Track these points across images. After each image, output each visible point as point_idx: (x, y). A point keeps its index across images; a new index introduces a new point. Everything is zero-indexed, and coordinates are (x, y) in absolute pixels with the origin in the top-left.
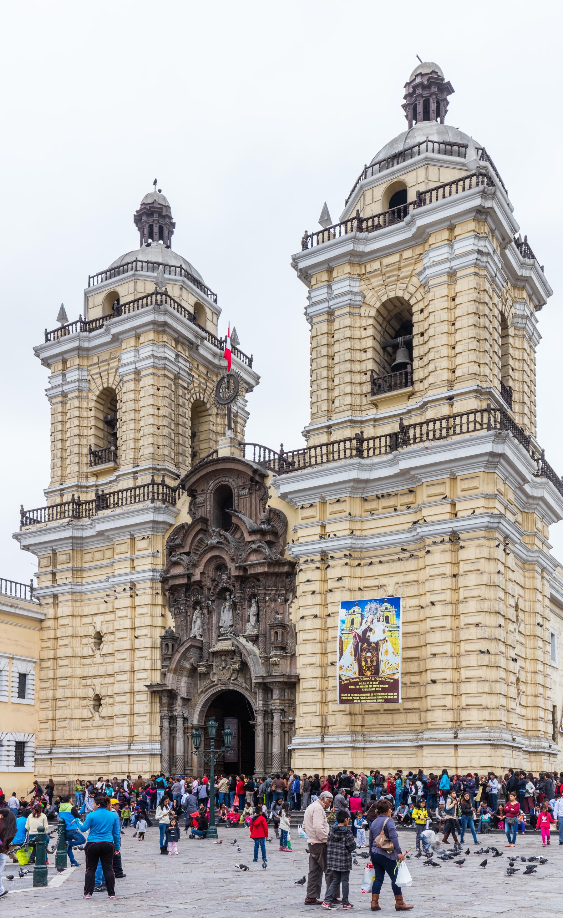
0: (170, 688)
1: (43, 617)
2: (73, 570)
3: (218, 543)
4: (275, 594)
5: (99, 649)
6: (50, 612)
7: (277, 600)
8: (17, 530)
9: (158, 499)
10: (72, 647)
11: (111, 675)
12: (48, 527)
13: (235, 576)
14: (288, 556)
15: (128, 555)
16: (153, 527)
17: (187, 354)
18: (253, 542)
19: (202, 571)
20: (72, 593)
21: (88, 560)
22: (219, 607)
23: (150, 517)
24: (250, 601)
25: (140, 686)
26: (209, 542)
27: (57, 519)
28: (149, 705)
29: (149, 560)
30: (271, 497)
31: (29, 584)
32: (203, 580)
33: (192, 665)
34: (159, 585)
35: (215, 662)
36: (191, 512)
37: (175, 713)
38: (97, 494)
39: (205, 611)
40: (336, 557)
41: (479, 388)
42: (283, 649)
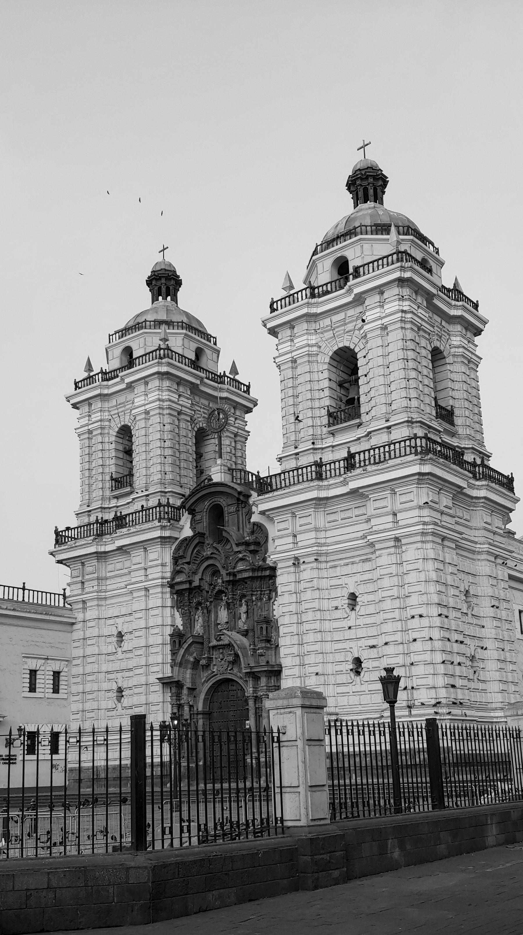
0: (176, 680)
1: (74, 621)
2: (98, 579)
3: (212, 554)
4: (261, 594)
5: (121, 647)
6: (80, 616)
7: (263, 599)
8: (52, 548)
9: (164, 518)
10: (98, 646)
11: (130, 670)
12: (77, 544)
13: (226, 581)
14: (269, 562)
15: (142, 565)
16: (161, 542)
17: (189, 393)
18: (240, 552)
19: (200, 578)
20: (99, 599)
21: (111, 570)
22: (216, 607)
23: (157, 533)
24: (241, 601)
25: (153, 679)
26: (205, 554)
27: (84, 537)
28: (162, 695)
29: (159, 569)
30: (254, 512)
31: (62, 592)
32: (202, 585)
33: (195, 658)
34: (168, 590)
35: (215, 655)
36: (193, 528)
37: (182, 702)
38: (116, 515)
39: (205, 611)
40: (306, 561)
41: (410, 419)
42: (269, 641)
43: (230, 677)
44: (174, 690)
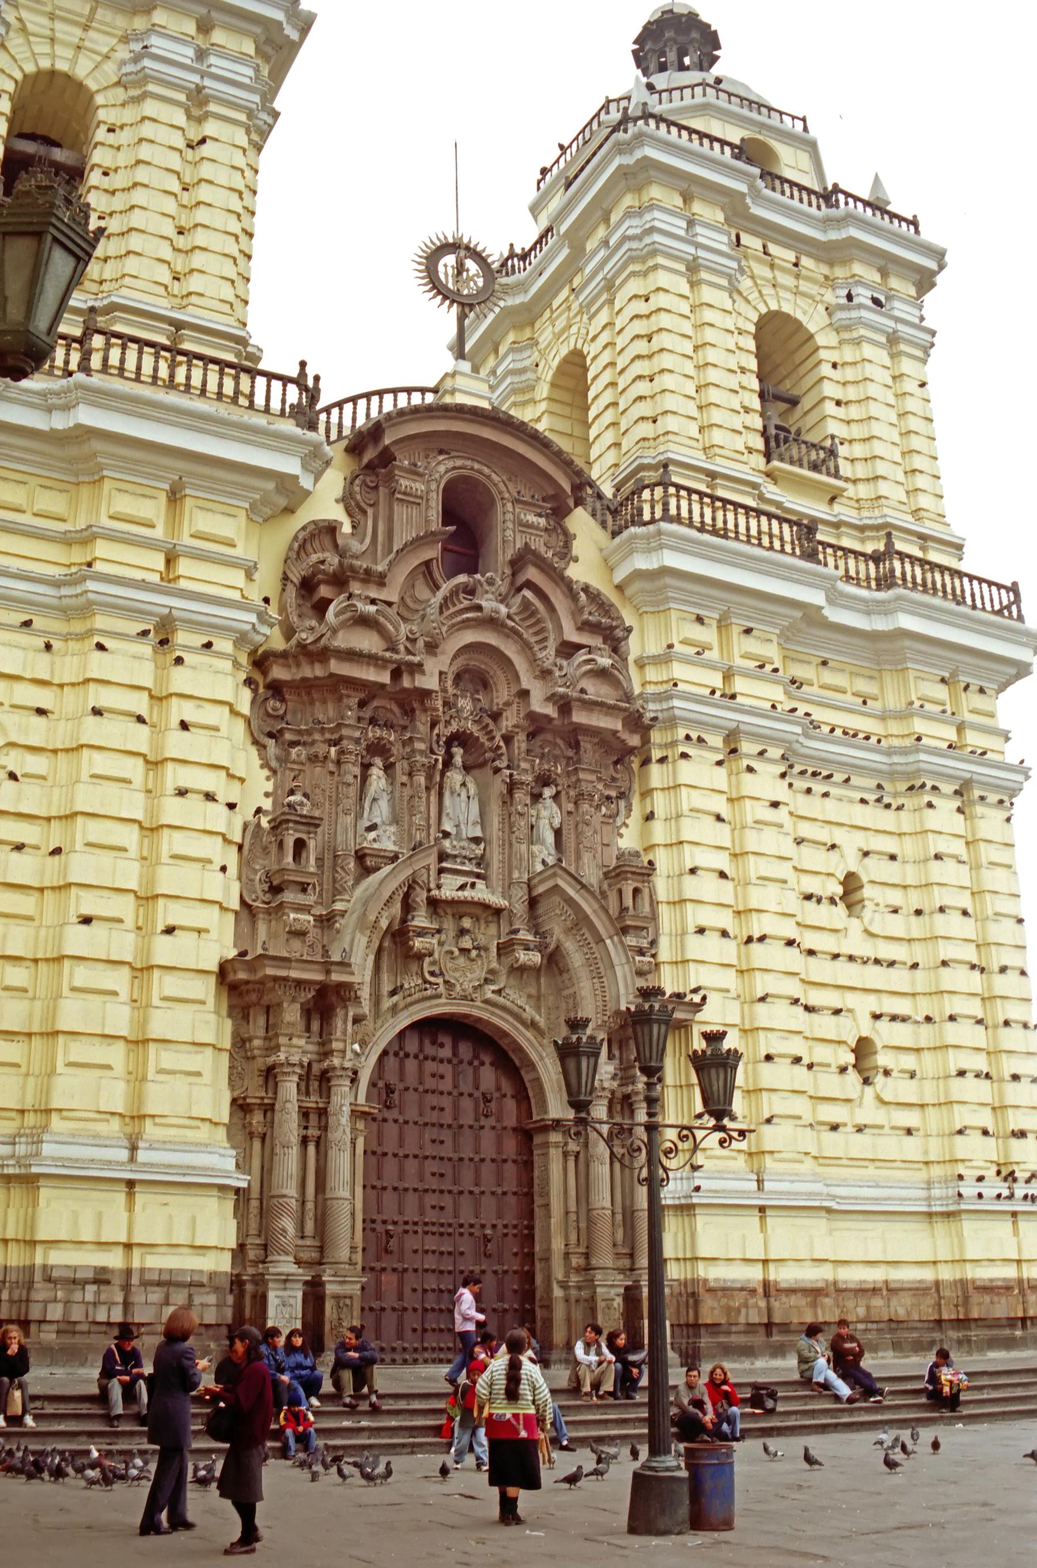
29: (237, 577)
43: (485, 1015)
44: (292, 1014)
